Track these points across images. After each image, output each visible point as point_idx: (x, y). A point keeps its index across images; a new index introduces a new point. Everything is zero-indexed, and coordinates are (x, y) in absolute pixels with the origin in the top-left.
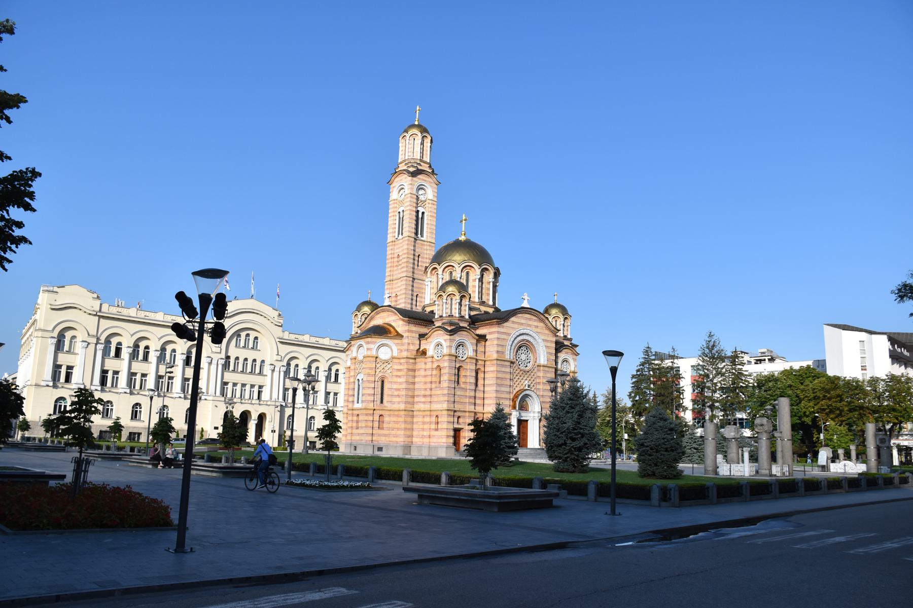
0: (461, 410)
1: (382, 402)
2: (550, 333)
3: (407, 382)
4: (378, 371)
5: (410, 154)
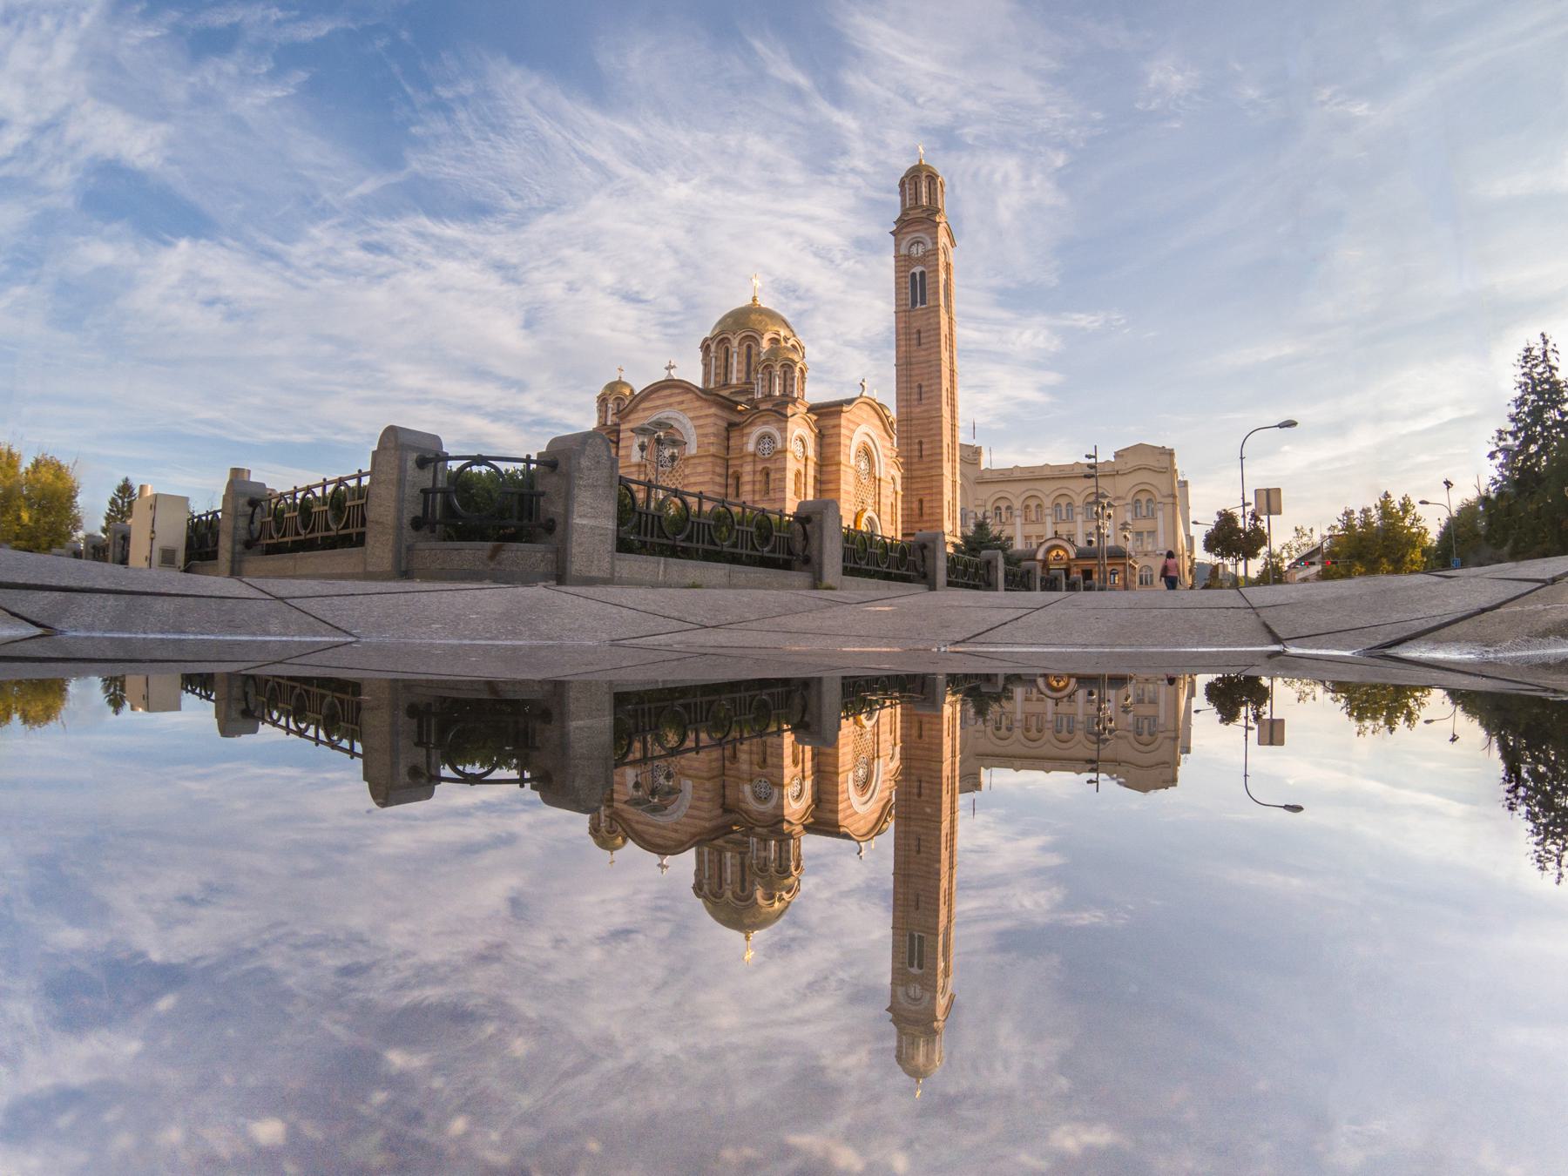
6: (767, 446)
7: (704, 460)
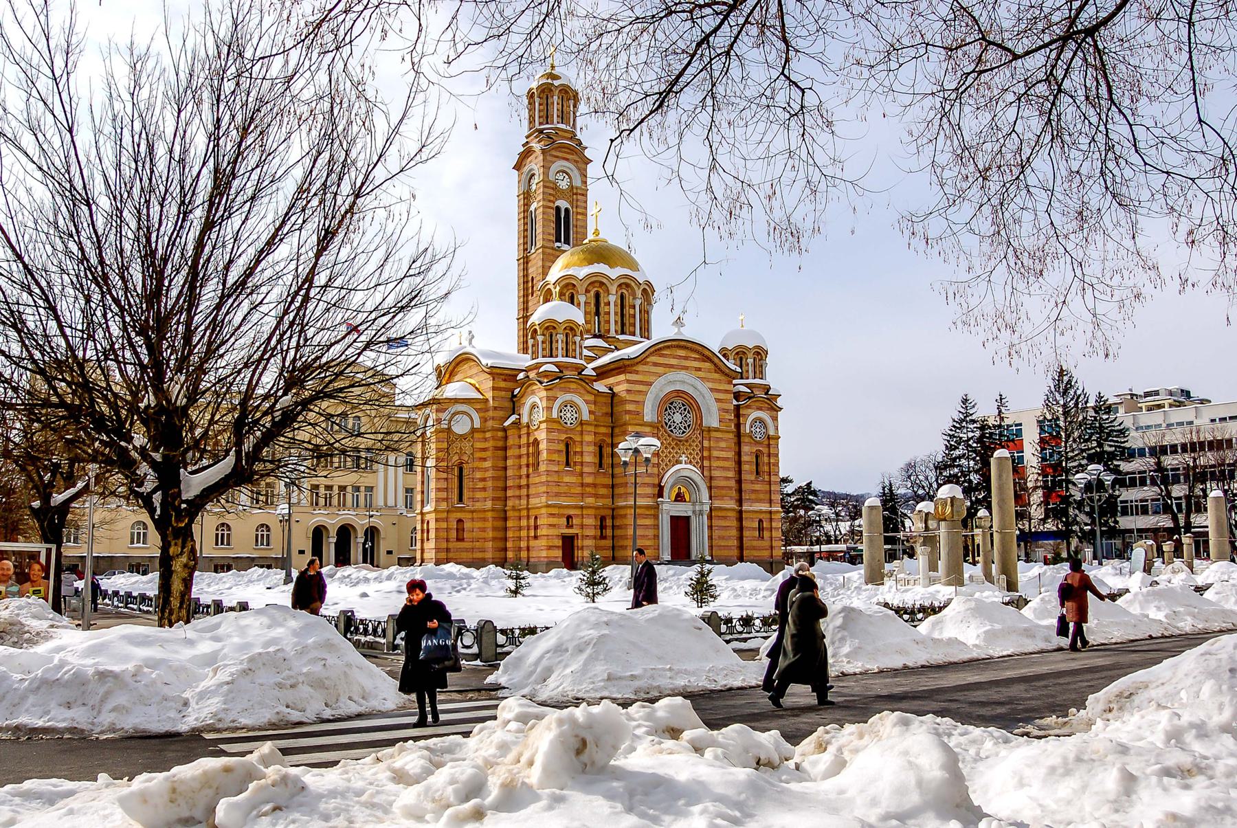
1: (461, 500)
3: (495, 468)
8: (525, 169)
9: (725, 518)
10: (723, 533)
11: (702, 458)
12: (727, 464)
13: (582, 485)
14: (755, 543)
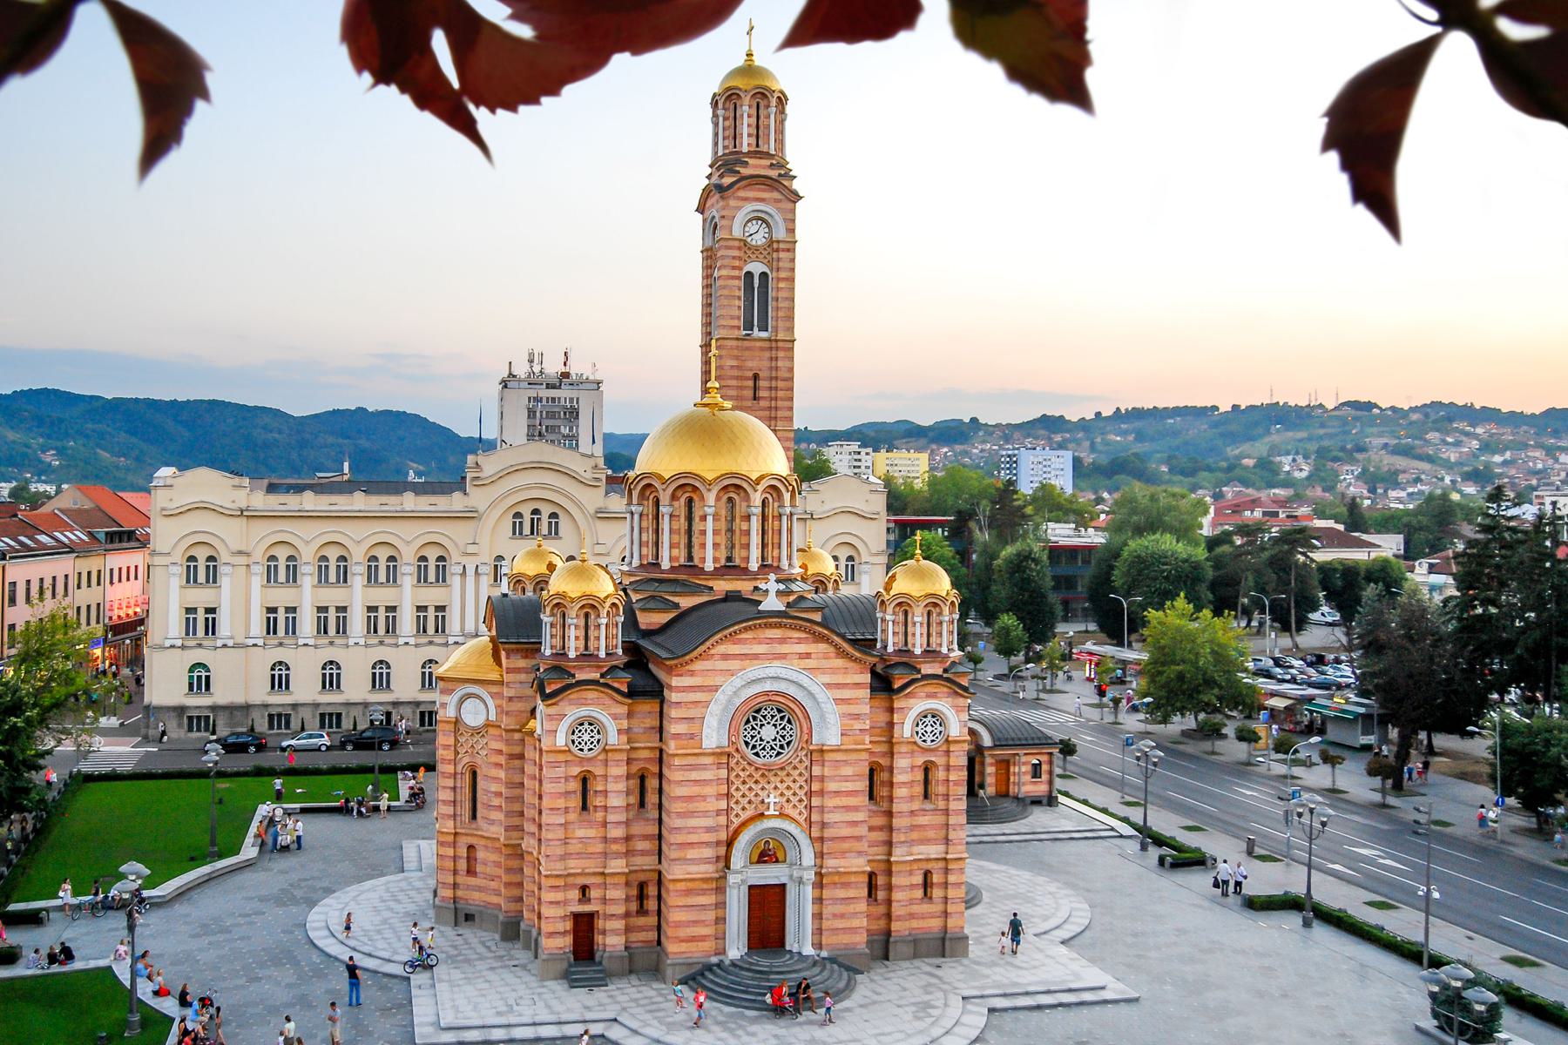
0: (587, 871)
2: (852, 664)
4: (462, 751)
5: (726, 143)
6: (929, 729)
7: (854, 756)
8: (707, 213)
9: (846, 885)
10: (839, 909)
11: (810, 794)
12: (852, 801)
13: (605, 839)
14: (915, 908)
